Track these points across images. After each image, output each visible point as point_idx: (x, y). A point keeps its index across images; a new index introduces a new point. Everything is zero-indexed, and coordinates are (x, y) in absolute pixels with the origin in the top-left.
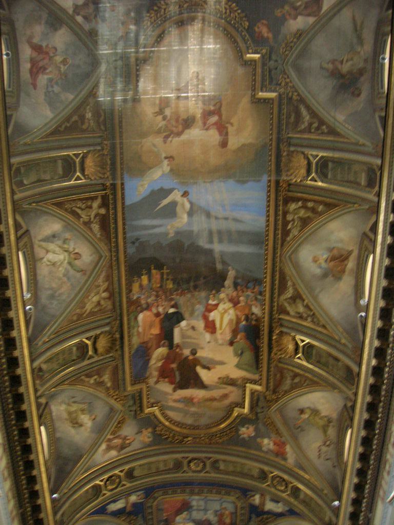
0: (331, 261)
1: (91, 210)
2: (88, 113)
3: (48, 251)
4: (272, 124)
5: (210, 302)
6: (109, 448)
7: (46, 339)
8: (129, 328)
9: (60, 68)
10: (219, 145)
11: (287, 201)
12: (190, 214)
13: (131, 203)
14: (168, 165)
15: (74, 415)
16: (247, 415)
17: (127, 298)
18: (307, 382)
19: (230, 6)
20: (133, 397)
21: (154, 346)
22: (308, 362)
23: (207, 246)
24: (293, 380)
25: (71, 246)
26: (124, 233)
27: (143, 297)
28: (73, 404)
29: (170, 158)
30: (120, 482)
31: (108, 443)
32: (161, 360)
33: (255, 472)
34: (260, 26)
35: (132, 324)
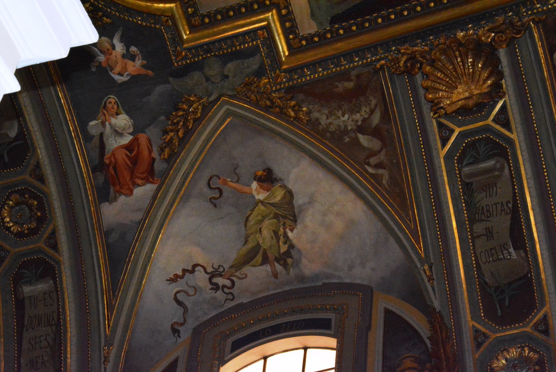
24: (362, 129)
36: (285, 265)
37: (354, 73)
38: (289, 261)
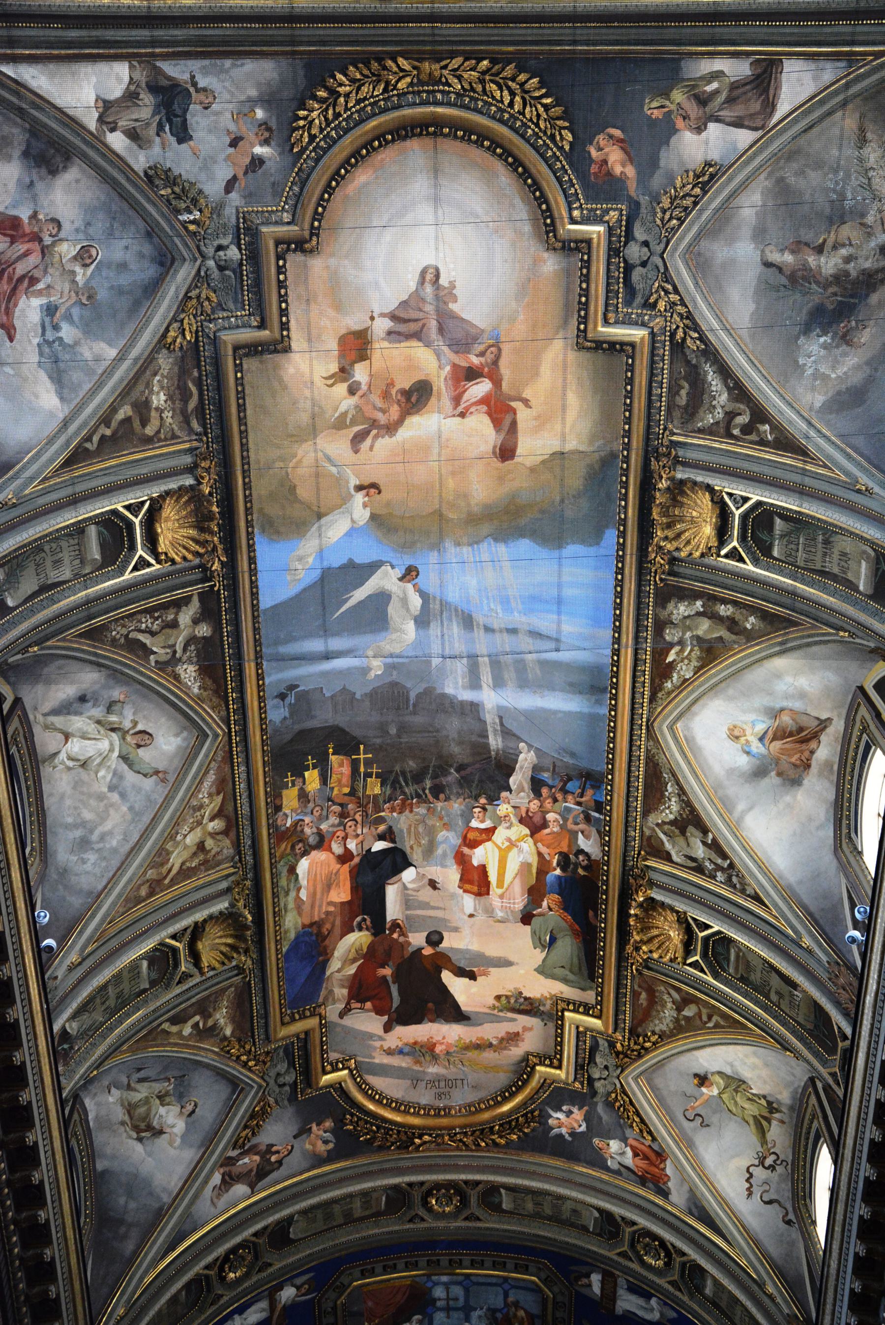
0: (774, 739)
1: (175, 632)
2: (158, 393)
3: (67, 736)
5: (474, 824)
6: (228, 1181)
7: (74, 957)
8: (275, 895)
9: (73, 273)
10: (494, 453)
11: (666, 595)
12: (422, 621)
13: (273, 603)
14: (365, 505)
15: (142, 1110)
18: (715, 1018)
19: (522, 85)
20: (288, 1051)
21: (337, 931)
22: (716, 976)
23: (466, 695)
24: (679, 1009)
25: (126, 718)
26: (260, 677)
27: (307, 819)
28: (138, 1086)
29: (370, 488)
30: (256, 1257)
31: (227, 1169)
32: (354, 960)
33: (590, 1219)
34: (602, 143)
35: (283, 882)
36: (778, 1111)
37: (636, 987)
38: (775, 1105)
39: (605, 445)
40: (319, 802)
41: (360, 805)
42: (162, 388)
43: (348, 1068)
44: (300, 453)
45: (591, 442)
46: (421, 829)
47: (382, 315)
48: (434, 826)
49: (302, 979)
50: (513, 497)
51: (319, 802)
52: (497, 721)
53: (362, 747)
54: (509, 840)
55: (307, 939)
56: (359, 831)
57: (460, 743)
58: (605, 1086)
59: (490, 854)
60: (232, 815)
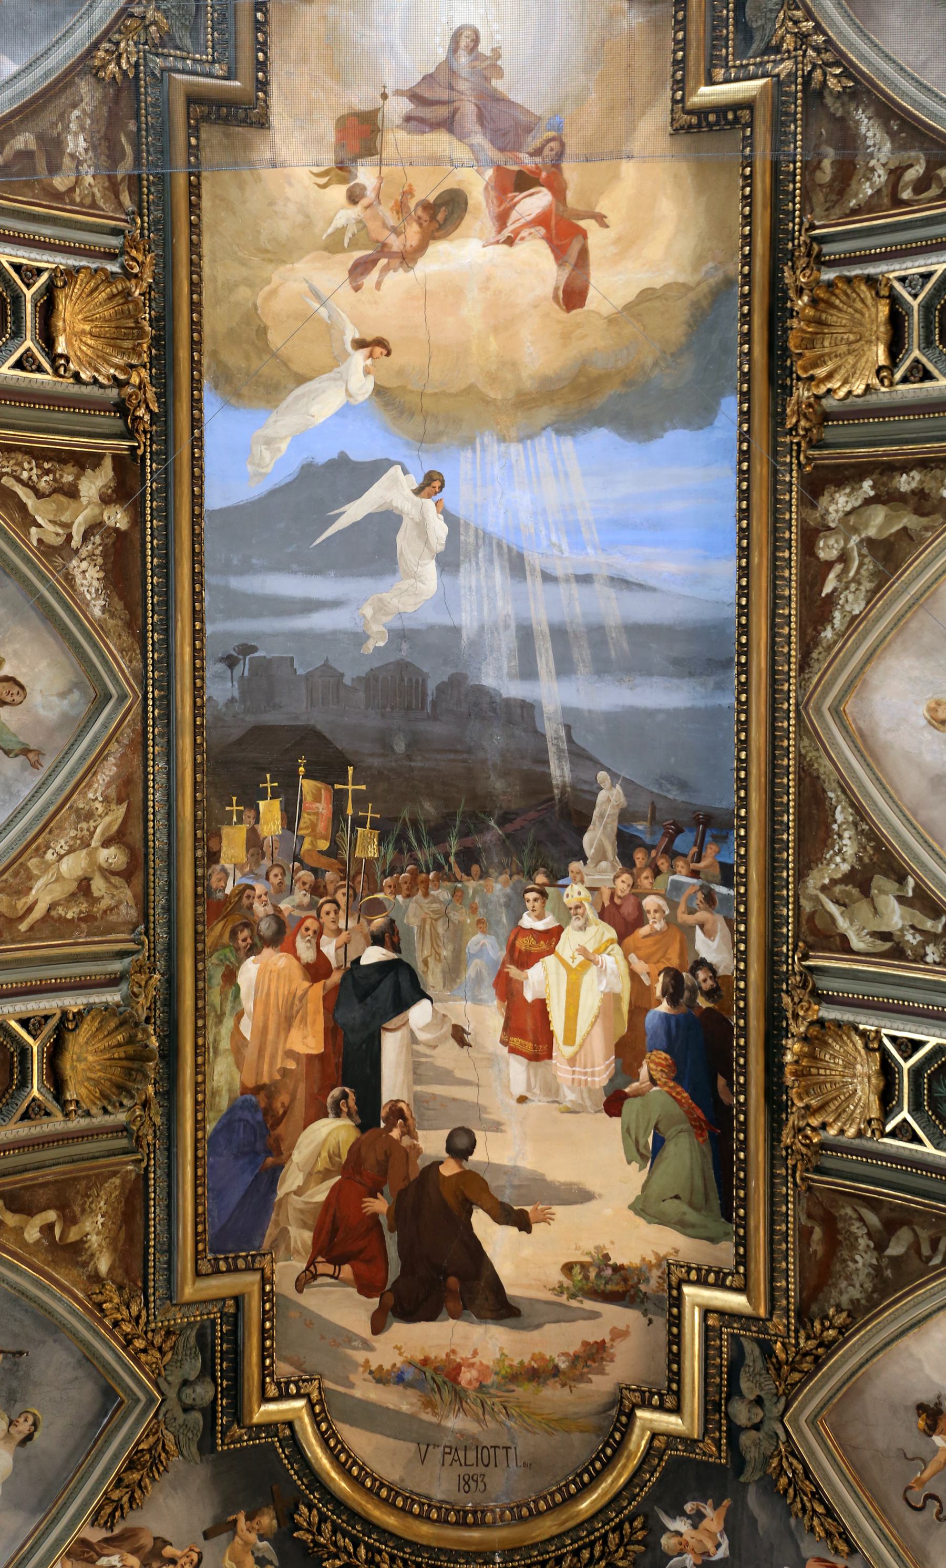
1: (73, 505)
2: (76, 135)
4: (748, 200)
5: (527, 921)
8: (199, 1012)
10: (556, 297)
13: (224, 504)
14: (367, 372)
16: (689, 1443)
17: (198, 881)
23: (514, 690)
27: (260, 888)
32: (326, 1175)
35: (214, 996)
39: (716, 268)
40: (279, 859)
41: (344, 874)
42: (82, 128)
43: (308, 1396)
44: (276, 279)
45: (695, 268)
46: (441, 930)
47: (398, 93)
48: (461, 924)
49: (235, 1195)
50: (584, 363)
51: (279, 859)
52: (563, 733)
53: (350, 770)
54: (583, 951)
55: (247, 1115)
56: (342, 925)
57: (505, 774)
58: (757, 1444)
59: (552, 979)
60: (139, 845)
